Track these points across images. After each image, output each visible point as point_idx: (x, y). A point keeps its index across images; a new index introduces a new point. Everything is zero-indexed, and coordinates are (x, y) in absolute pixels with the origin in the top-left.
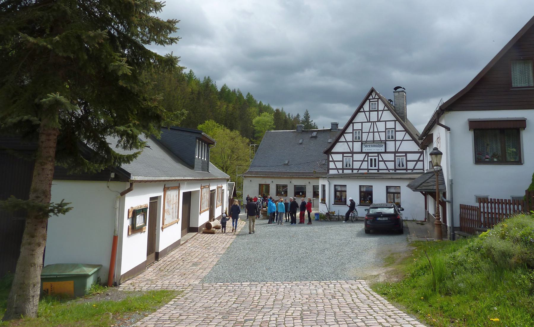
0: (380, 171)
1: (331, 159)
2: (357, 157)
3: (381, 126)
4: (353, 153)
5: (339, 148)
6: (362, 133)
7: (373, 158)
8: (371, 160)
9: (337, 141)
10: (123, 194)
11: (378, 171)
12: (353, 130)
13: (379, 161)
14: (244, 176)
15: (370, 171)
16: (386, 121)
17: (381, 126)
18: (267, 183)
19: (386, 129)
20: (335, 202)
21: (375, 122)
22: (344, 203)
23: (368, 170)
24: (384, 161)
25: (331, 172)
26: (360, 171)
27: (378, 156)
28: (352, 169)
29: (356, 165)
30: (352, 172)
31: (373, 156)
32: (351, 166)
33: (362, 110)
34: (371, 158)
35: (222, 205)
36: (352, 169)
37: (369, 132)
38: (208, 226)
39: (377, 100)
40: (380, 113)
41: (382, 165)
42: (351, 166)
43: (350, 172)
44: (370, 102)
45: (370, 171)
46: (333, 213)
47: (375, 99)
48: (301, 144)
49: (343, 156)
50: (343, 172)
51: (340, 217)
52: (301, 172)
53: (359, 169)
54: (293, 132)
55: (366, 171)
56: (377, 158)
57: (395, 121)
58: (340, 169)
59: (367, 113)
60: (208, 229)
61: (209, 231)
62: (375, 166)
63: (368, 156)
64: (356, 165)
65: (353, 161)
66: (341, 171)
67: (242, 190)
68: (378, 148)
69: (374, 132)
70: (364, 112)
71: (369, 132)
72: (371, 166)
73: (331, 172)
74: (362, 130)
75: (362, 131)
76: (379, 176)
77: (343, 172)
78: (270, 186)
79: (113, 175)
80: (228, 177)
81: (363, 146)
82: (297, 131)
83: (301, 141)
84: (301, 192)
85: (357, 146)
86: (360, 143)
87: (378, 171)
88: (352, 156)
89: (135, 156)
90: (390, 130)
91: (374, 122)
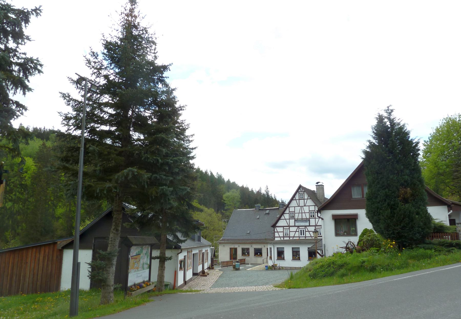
0: (307, 238)
1: (276, 231)
2: (292, 229)
3: (306, 209)
4: (289, 226)
5: (281, 223)
6: (295, 213)
7: (302, 229)
8: (301, 231)
9: (279, 219)
10: (178, 254)
11: (305, 238)
12: (289, 212)
13: (306, 231)
14: (220, 243)
15: (301, 238)
16: (309, 206)
17: (306, 209)
18: (236, 247)
19: (309, 211)
20: (277, 258)
21: (303, 206)
23: (299, 237)
25: (276, 239)
26: (294, 238)
27: (305, 228)
28: (290, 237)
29: (292, 234)
32: (289, 235)
33: (294, 199)
34: (301, 229)
35: (208, 262)
36: (290, 237)
37: (299, 213)
38: (203, 272)
39: (303, 192)
40: (306, 201)
42: (289, 235)
44: (299, 193)
45: (301, 238)
46: (276, 265)
47: (302, 191)
49: (283, 229)
50: (284, 239)
53: (294, 237)
55: (298, 238)
56: (304, 229)
57: (315, 206)
58: (282, 237)
59: (298, 201)
60: (203, 273)
62: (304, 235)
63: (299, 228)
64: (292, 234)
65: (290, 232)
66: (282, 239)
67: (218, 252)
68: (305, 223)
69: (302, 213)
70: (296, 200)
71: (299, 213)
72: (301, 235)
73: (276, 239)
74: (294, 212)
75: (295, 212)
77: (284, 239)
79: (174, 247)
80: (210, 243)
81: (296, 222)
82: (255, 209)
83: (258, 217)
85: (292, 222)
87: (305, 238)
88: (289, 229)
90: (312, 212)
91: (302, 206)
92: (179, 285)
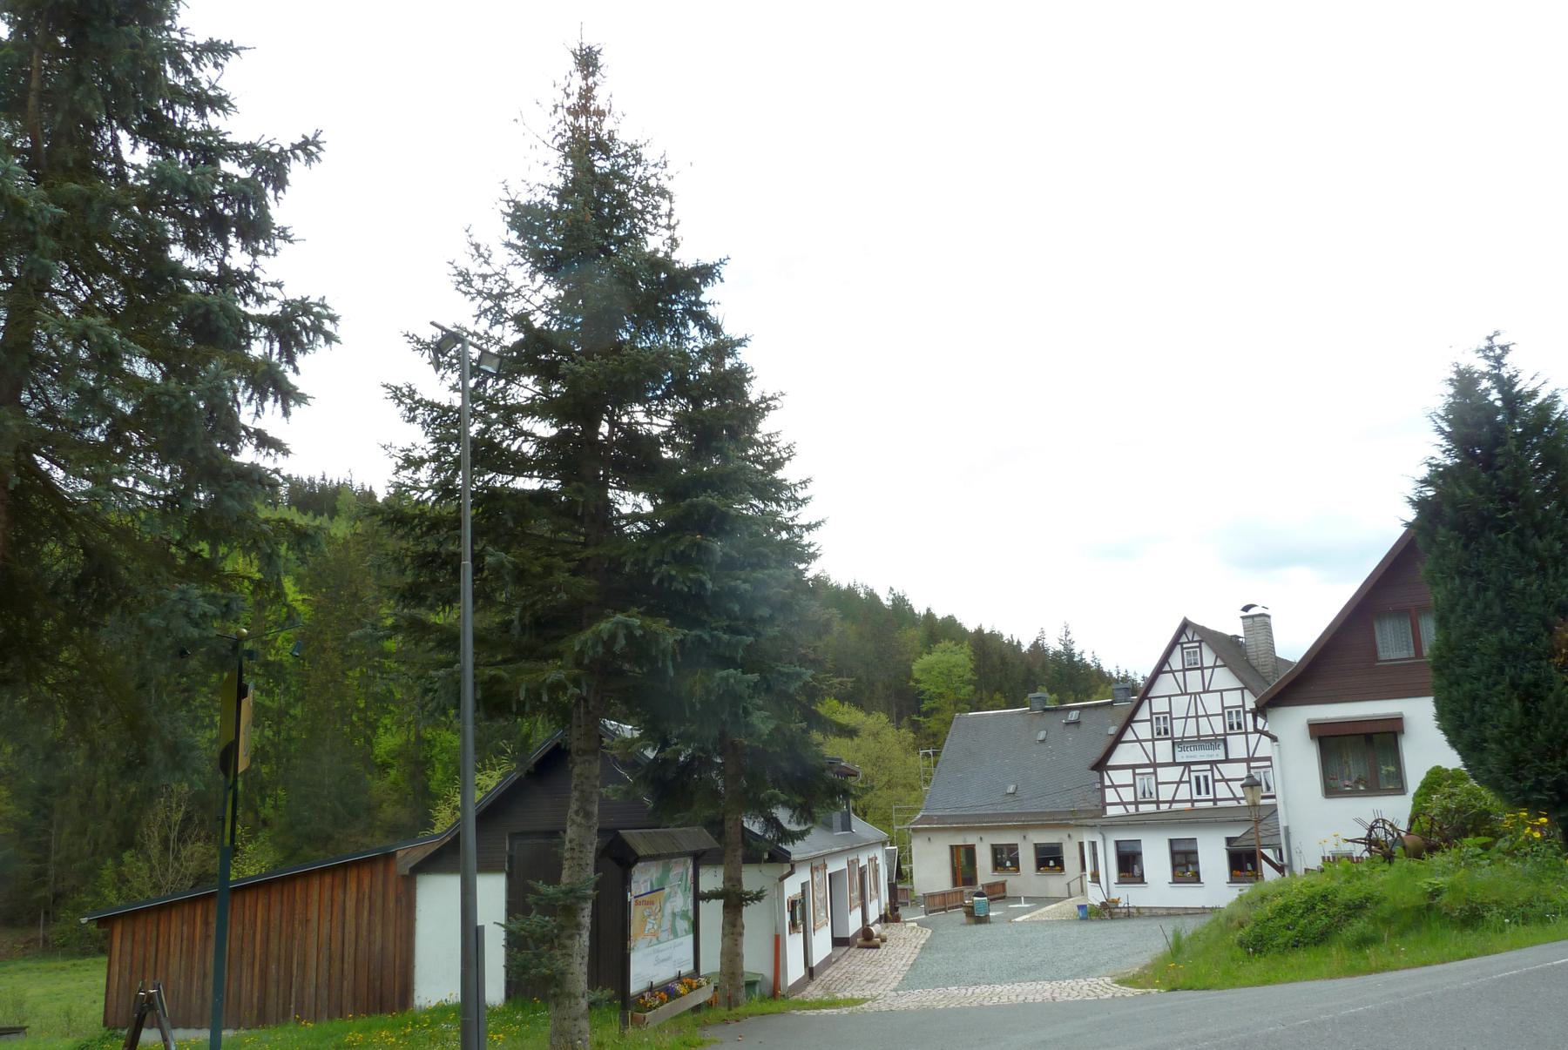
0: (1220, 804)
1: (1107, 782)
2: (1165, 774)
3: (1212, 703)
4: (1155, 765)
5: (1122, 755)
6: (1172, 719)
7: (1201, 775)
8: (1197, 778)
9: (1118, 740)
10: (782, 879)
11: (1215, 804)
12: (1152, 714)
13: (1214, 781)
14: (913, 829)
15: (1197, 805)
16: (1221, 691)
17: (1212, 703)
18: (969, 842)
19: (1224, 708)
20: (1119, 877)
21: (1199, 693)
22: (1139, 880)
23: (1193, 801)
24: (1226, 781)
25: (1111, 811)
26: (1176, 806)
27: (1212, 770)
28: (1158, 802)
29: (1166, 793)
30: (1158, 808)
31: (1201, 771)
32: (1154, 795)
33: (1167, 668)
34: (1197, 774)
35: (879, 898)
36: (1158, 802)
37: (1187, 718)
38: (866, 934)
39: (1197, 644)
40: (1208, 673)
41: (1222, 791)
42: (1154, 795)
43: (1152, 808)
44: (1183, 649)
45: (1197, 805)
46: (1116, 902)
47: (1193, 642)
48: (1043, 741)
49: (1134, 774)
50: (1137, 809)
51: (1131, 910)
52: (1048, 810)
53: (1173, 801)
54: (1021, 713)
55: (1188, 805)
56: (1209, 774)
57: (1242, 689)
58: (1130, 803)
59: (1179, 675)
60: (867, 939)
61: (870, 943)
62: (1208, 793)
63: (1190, 771)
64: (1166, 793)
65: (1157, 784)
66: (1132, 809)
67: (911, 862)
68: (1211, 752)
69: (1197, 717)
70: (1172, 672)
71: (1187, 718)
72: (1199, 793)
73: (1111, 811)
74: (1170, 713)
75: (1171, 716)
76: (1212, 818)
77: (1137, 809)
78: (978, 850)
79: (766, 856)
80: (884, 835)
81: (1177, 749)
82: (1030, 710)
83: (1042, 735)
84: (1051, 859)
85: (1163, 751)
86: (1170, 742)
87: (1215, 804)
88: (1155, 773)
89: (806, 832)
90: (1234, 710)
91: (1195, 694)
92: (789, 984)
